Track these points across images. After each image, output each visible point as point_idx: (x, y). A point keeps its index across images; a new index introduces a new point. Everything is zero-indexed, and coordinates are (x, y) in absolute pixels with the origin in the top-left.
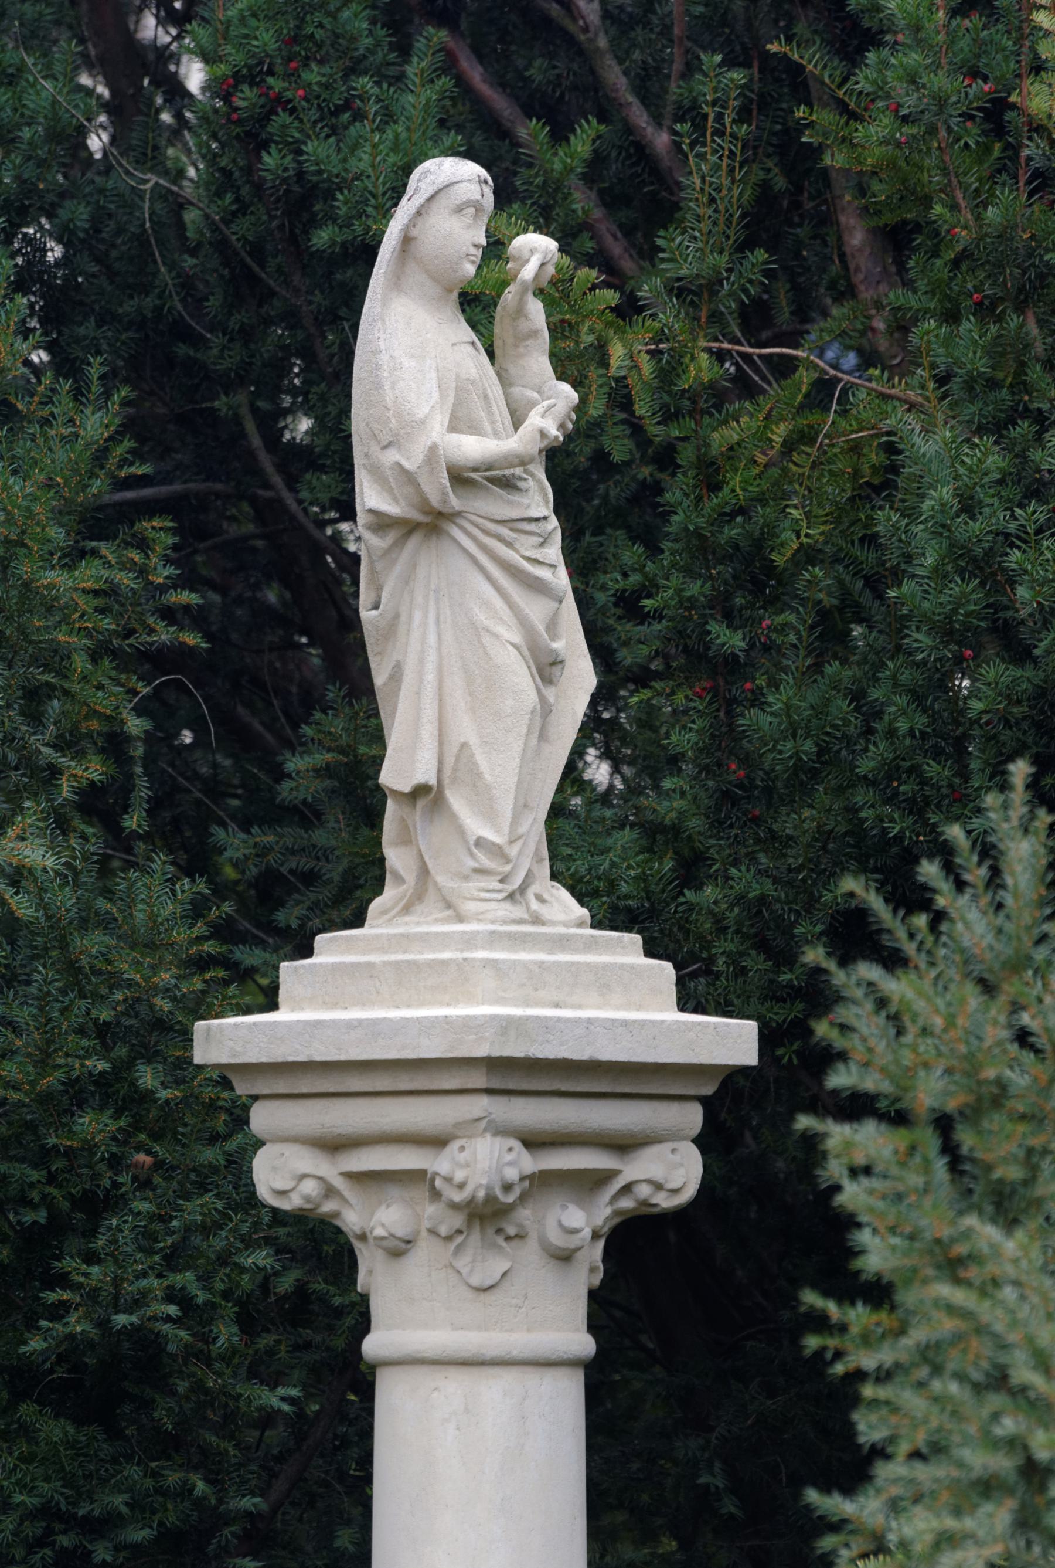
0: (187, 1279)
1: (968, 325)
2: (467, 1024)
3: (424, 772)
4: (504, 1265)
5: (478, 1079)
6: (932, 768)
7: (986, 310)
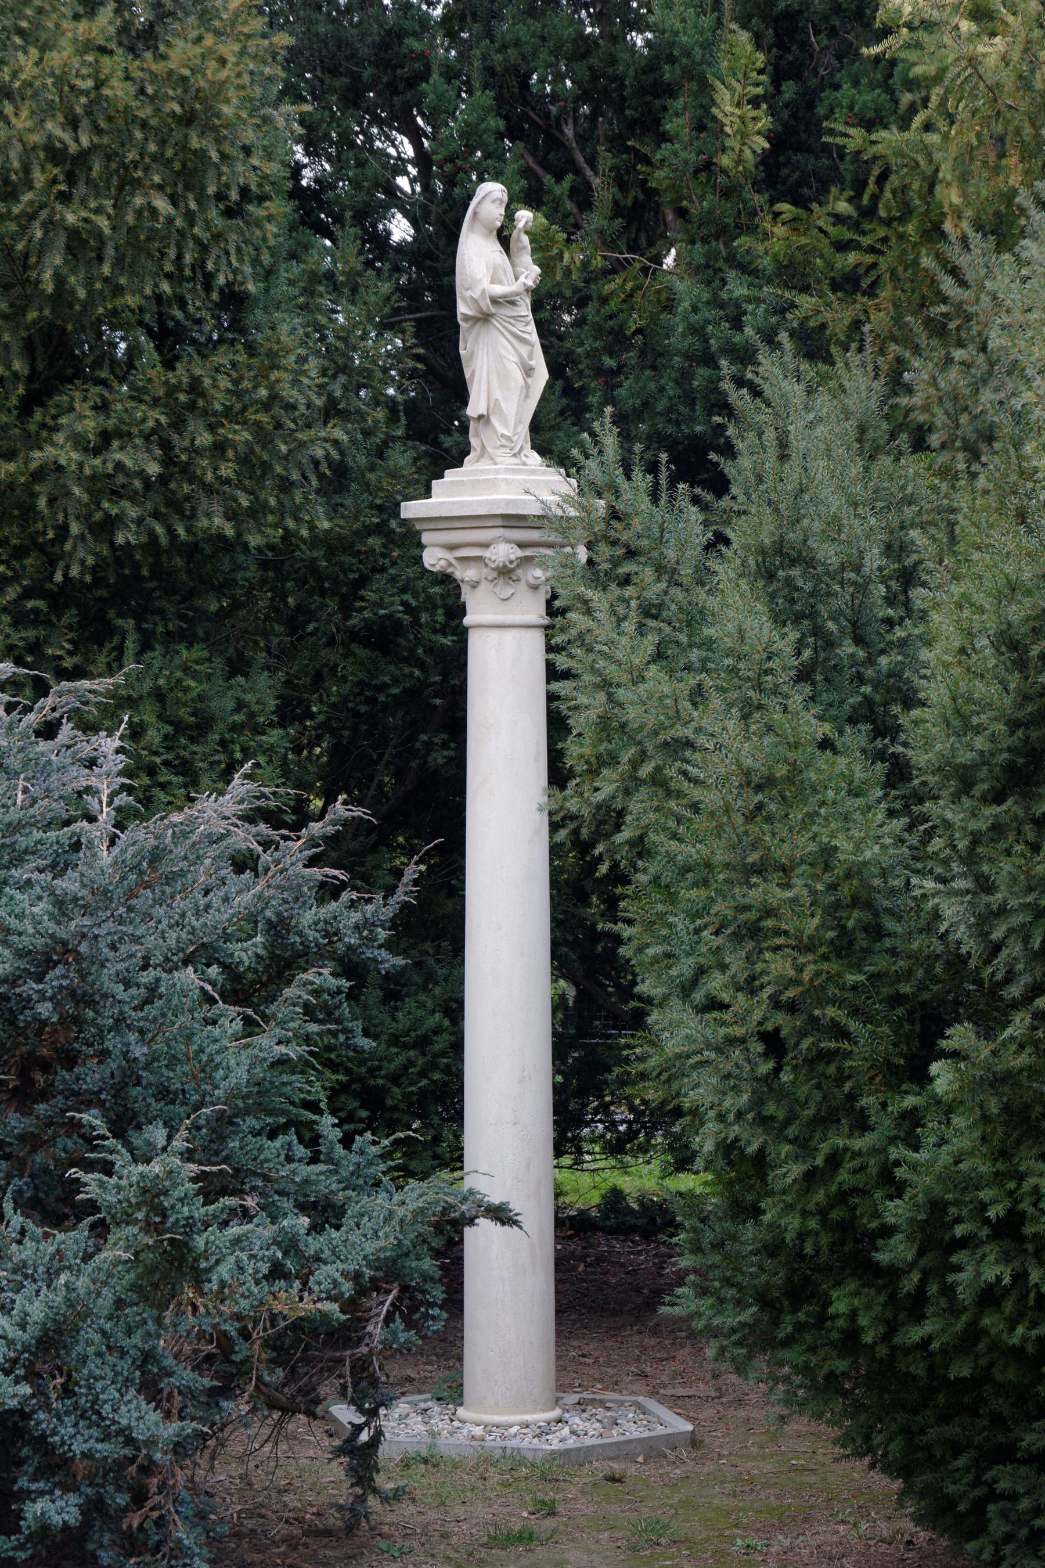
0: (407, 597)
1: (698, 245)
2: (495, 502)
3: (482, 410)
4: (510, 591)
5: (499, 522)
6: (681, 408)
7: (705, 240)
